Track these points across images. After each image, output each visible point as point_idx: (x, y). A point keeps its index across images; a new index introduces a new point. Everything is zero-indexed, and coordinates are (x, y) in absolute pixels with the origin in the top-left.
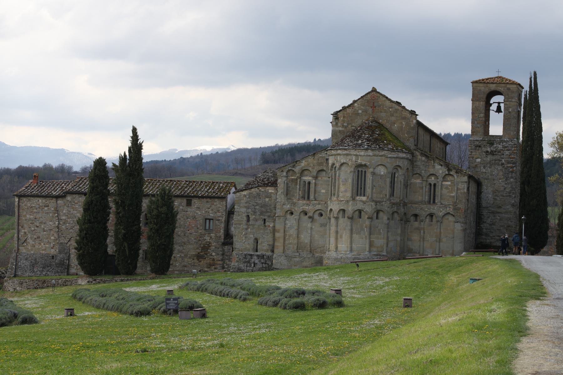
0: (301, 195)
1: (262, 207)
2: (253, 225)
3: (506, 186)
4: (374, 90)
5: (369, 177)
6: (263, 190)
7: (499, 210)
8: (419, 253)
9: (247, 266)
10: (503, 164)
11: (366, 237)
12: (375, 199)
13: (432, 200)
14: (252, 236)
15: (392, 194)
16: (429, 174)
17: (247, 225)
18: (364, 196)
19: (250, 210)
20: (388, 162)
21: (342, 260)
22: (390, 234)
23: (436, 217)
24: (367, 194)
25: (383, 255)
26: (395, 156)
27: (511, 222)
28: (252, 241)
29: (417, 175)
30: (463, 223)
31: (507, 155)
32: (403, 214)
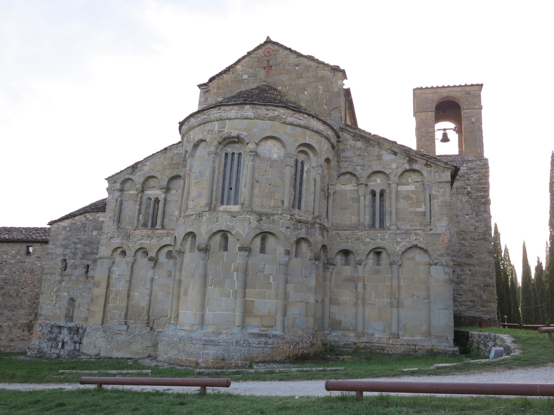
0: (142, 221)
1: (86, 245)
2: (70, 275)
3: (477, 224)
4: (268, 41)
5: (247, 162)
6: (91, 218)
7: (468, 261)
8: (355, 330)
9: (51, 347)
10: (469, 193)
11: (235, 292)
12: (257, 209)
13: (378, 221)
14: (66, 294)
15: (297, 202)
16: (370, 172)
17: (62, 275)
18: (236, 203)
19: (68, 251)
20: (286, 133)
21: (181, 346)
22: (290, 287)
23: (389, 255)
24: (241, 199)
25: (274, 336)
26: (302, 123)
27: (491, 278)
28: (64, 303)
29: (348, 176)
30: (447, 266)
31: (475, 179)
32: (319, 246)
